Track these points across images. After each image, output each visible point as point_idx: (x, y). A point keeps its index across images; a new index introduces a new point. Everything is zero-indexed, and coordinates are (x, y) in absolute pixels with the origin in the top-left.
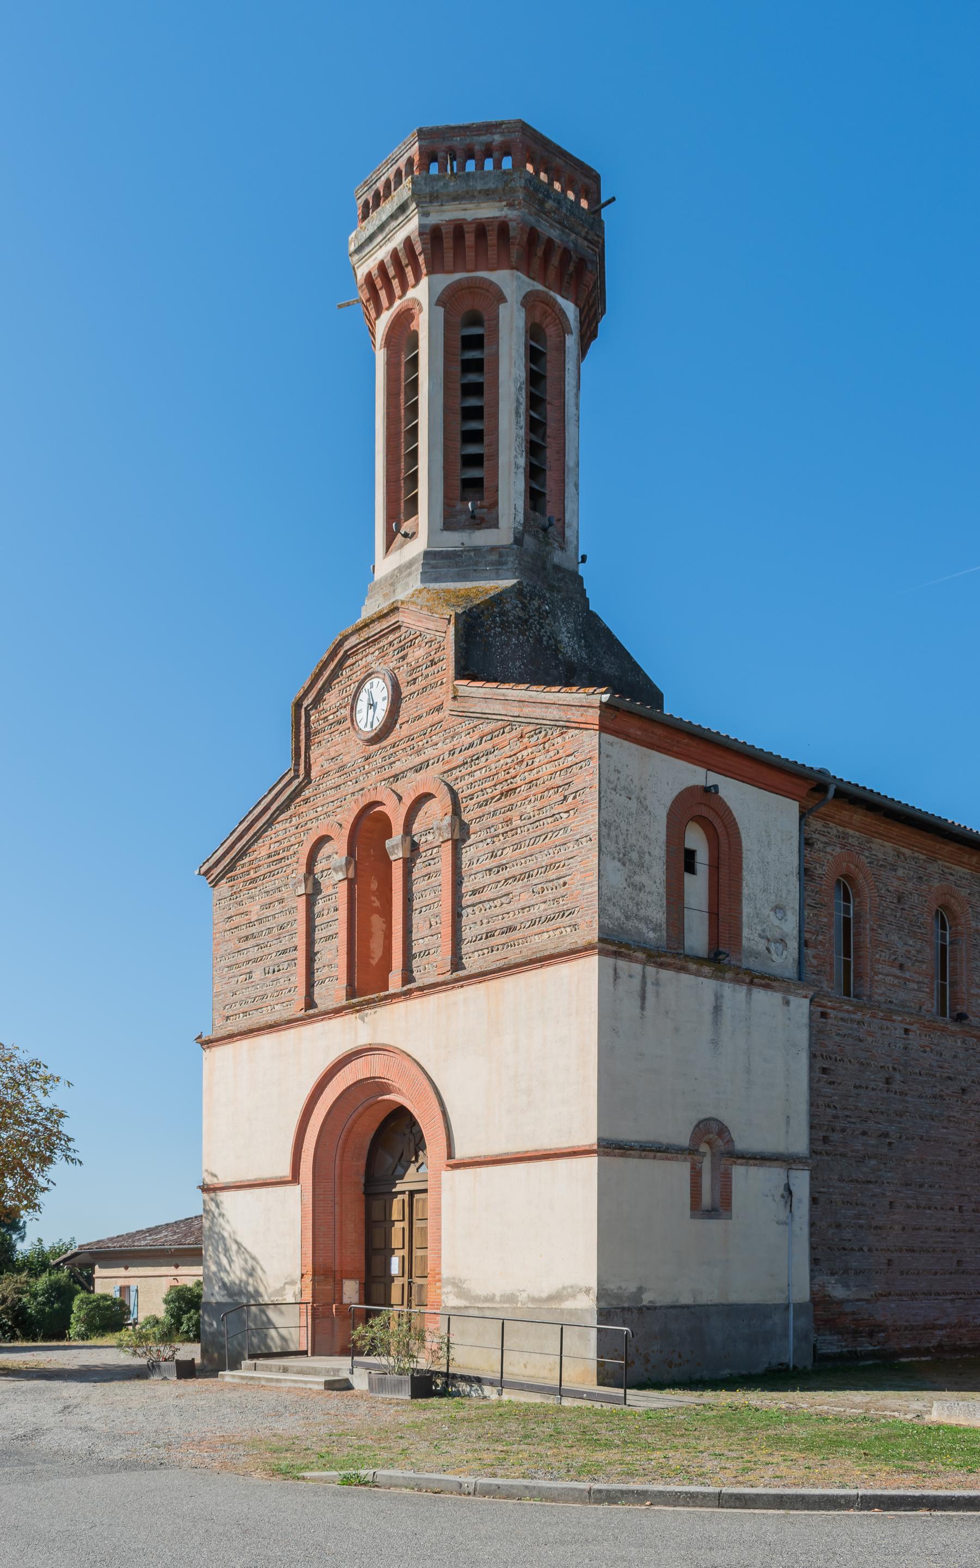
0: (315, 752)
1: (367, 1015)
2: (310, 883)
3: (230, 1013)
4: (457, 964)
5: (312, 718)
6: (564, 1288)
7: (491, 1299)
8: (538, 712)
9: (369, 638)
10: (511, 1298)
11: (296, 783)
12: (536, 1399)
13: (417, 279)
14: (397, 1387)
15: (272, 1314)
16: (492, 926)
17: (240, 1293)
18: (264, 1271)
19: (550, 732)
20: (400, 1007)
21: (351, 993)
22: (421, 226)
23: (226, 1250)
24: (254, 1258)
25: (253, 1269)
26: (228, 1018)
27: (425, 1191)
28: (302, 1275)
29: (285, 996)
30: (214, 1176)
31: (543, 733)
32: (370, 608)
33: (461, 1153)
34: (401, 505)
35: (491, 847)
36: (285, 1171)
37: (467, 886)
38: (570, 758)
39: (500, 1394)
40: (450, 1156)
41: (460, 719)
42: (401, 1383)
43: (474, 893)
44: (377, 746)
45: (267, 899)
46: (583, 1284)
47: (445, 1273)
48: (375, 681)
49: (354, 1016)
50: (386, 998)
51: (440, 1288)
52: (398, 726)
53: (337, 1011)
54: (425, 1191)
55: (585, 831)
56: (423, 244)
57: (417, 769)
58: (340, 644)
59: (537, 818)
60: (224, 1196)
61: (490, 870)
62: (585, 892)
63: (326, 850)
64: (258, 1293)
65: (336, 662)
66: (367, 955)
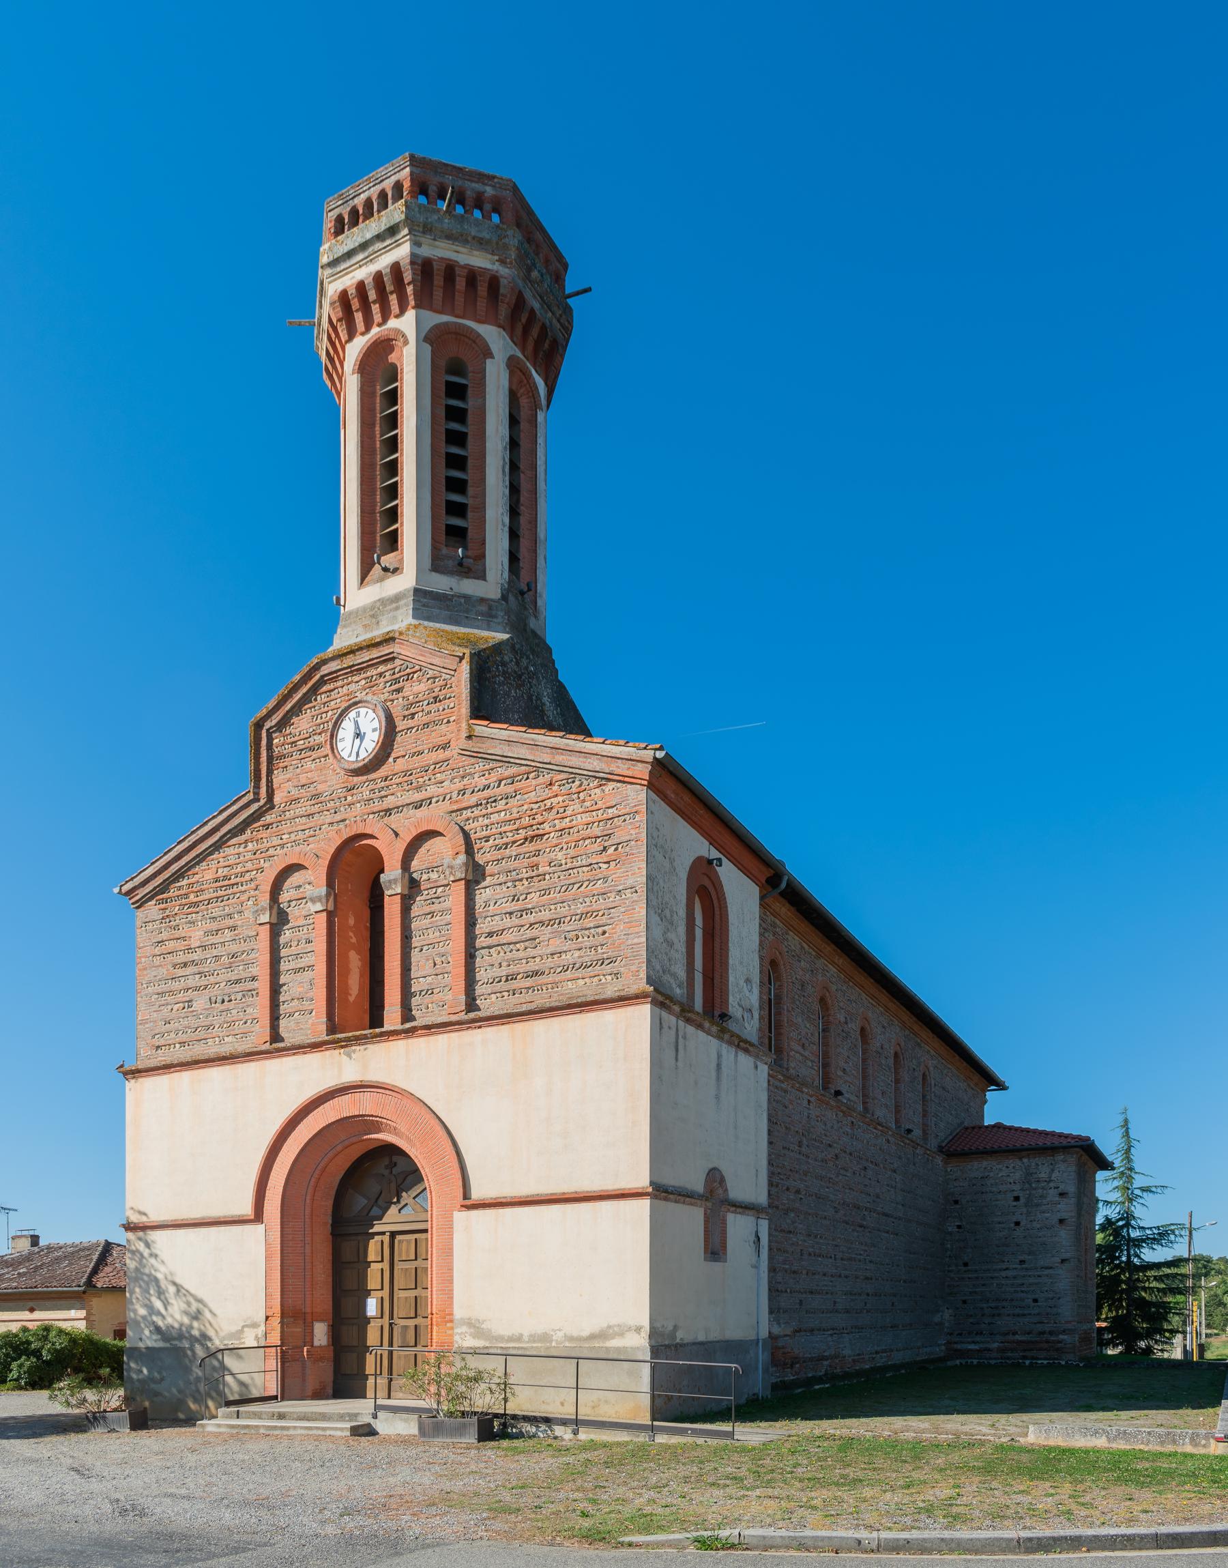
0: (278, 778)
1: (354, 1051)
2: (275, 911)
3: (162, 1042)
4: (471, 1005)
5: (275, 741)
6: (609, 1327)
7: (519, 1338)
8: (575, 761)
10: (545, 1337)
11: (255, 806)
12: (623, 1437)
13: (403, 310)
14: (460, 1431)
15: (229, 1361)
16: (513, 969)
17: (181, 1336)
18: (214, 1315)
19: (585, 783)
20: (399, 1046)
21: (332, 1028)
22: (413, 255)
23: (161, 1293)
24: (200, 1301)
25: (199, 1312)
26: (158, 1047)
27: (426, 1231)
28: (267, 1318)
29: (239, 1027)
30: (145, 1214)
31: (577, 783)
32: (343, 639)
33: (477, 1194)
34: (380, 538)
35: (513, 891)
36: (247, 1209)
37: (482, 927)
38: (610, 811)
39: (575, 1433)
40: (466, 1195)
41: (473, 760)
42: (464, 1426)
43: (490, 935)
44: (365, 778)
45: (215, 926)
46: (632, 1323)
47: (459, 1312)
48: (363, 711)
49: (337, 1051)
50: (382, 1034)
51: (452, 1328)
52: (391, 760)
53: (316, 1046)
54: (426, 1231)
55: (630, 882)
56: (414, 274)
57: (418, 805)
58: (316, 668)
59: (568, 866)
60: (154, 1236)
61: (511, 913)
62: (630, 942)
63: (295, 878)
64: (205, 1336)
65: (312, 685)
66: (345, 991)
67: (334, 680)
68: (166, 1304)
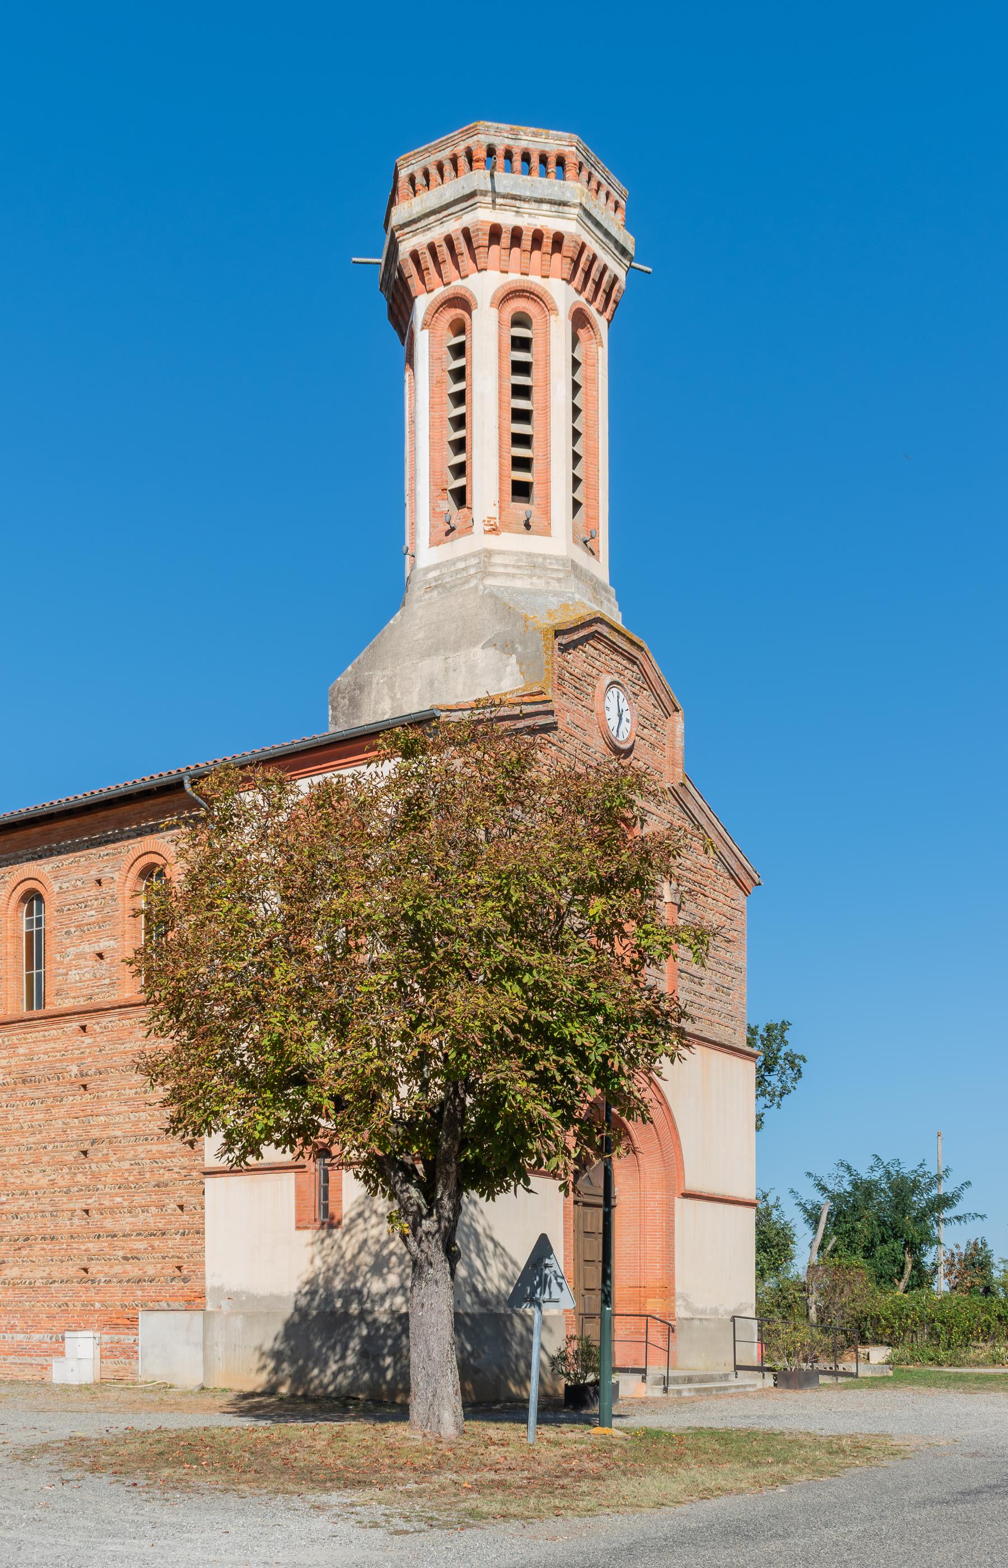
9: (614, 643)
23: (480, 1251)
41: (675, 802)
67: (600, 641)
68: (486, 1264)
